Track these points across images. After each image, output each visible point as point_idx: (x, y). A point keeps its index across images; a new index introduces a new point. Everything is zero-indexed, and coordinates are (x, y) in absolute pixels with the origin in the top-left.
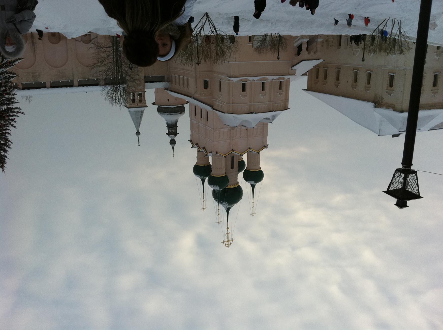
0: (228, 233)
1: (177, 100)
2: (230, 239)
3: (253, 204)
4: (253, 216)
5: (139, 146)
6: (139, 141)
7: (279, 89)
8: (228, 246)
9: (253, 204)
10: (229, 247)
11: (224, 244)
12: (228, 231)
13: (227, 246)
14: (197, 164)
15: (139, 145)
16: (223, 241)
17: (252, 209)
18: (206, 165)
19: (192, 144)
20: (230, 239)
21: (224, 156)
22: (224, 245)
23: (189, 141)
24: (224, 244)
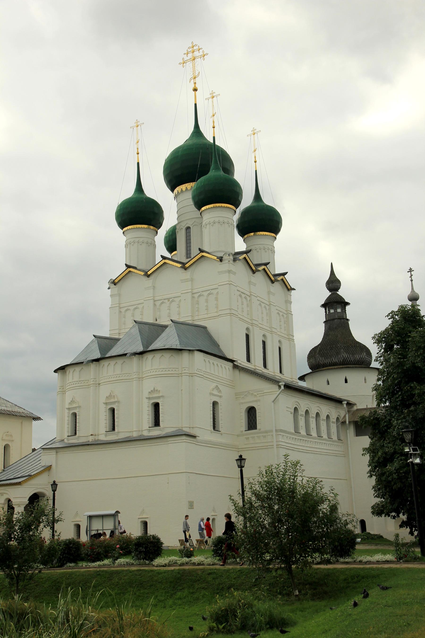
1: (326, 383)
2: (189, 65)
3: (138, 148)
4: (137, 121)
5: (411, 269)
6: (412, 281)
7: (77, 414)
9: (138, 148)
10: (191, 45)
11: (203, 51)
13: (195, 48)
14: (273, 235)
15: (411, 270)
18: (252, 234)
19: (284, 283)
21: (204, 254)
23: (294, 289)
24: (203, 51)
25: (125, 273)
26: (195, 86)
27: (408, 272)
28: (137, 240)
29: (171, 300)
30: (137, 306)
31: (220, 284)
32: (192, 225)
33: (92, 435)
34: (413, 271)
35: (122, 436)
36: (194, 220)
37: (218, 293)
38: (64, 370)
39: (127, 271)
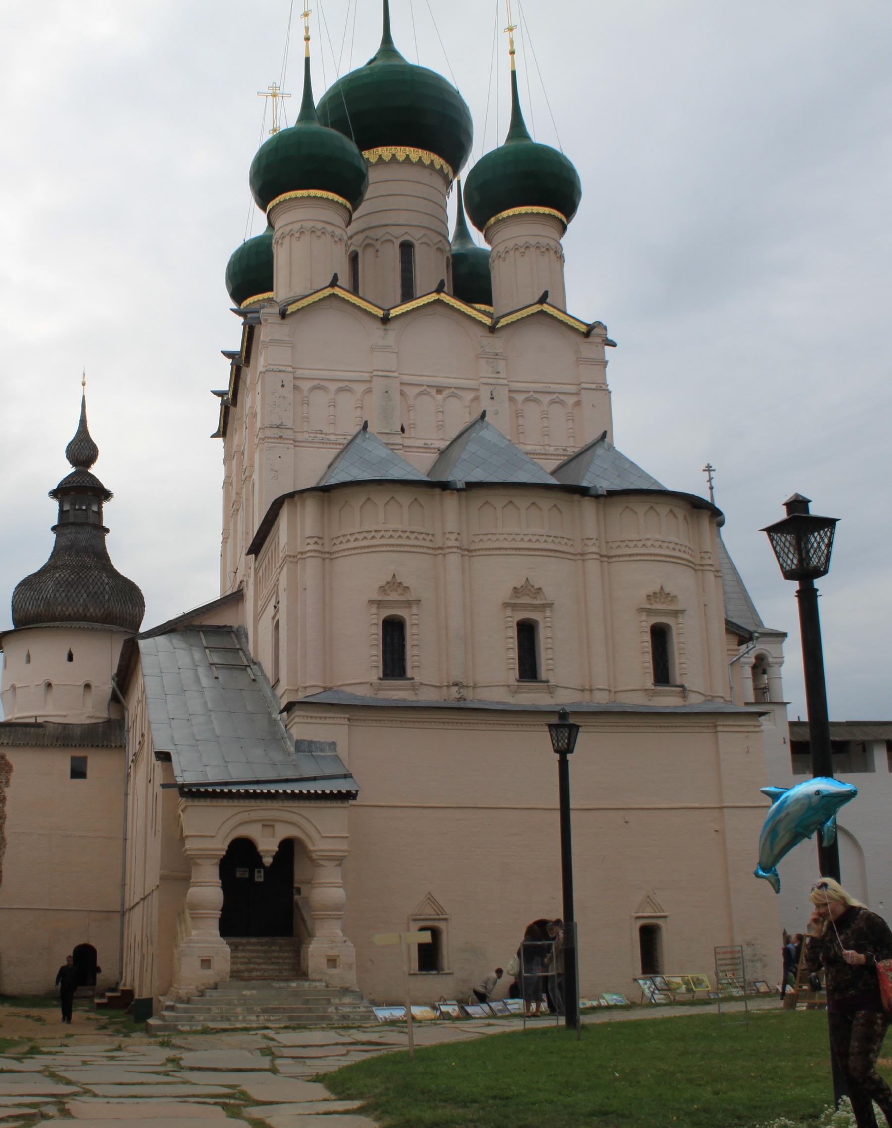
6: (711, 488)
15: (709, 469)
27: (704, 471)
28: (329, 228)
29: (445, 393)
30: (347, 383)
31: (584, 385)
32: (420, 242)
34: (714, 471)
36: (424, 232)
37: (578, 404)
38: (326, 494)
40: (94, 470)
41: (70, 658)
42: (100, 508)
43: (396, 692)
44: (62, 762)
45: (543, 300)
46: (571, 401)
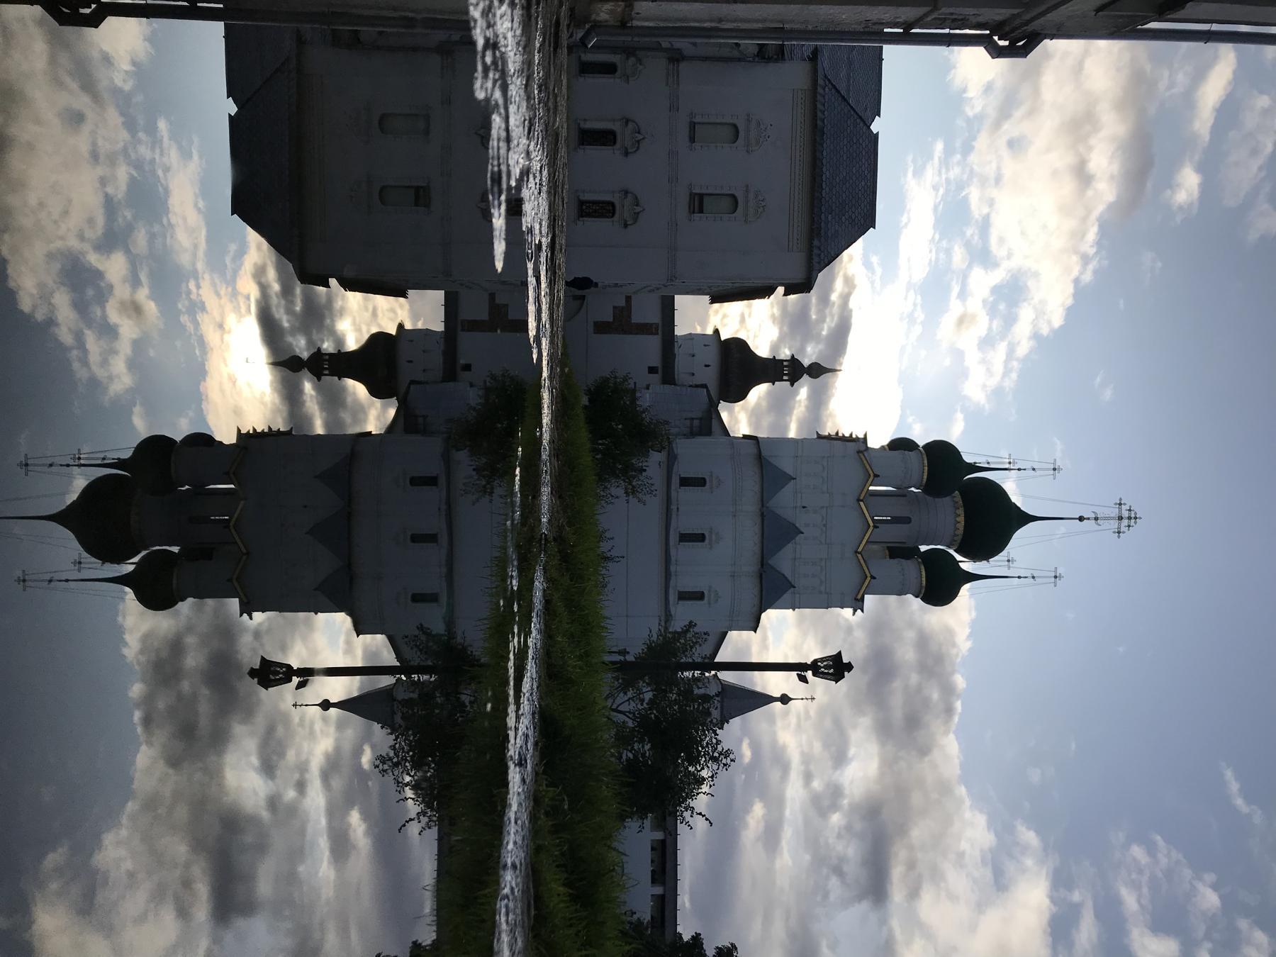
0: (1096, 519)
3: (1025, 469)
4: (1060, 469)
6: (802, 699)
8: (1136, 518)
11: (1124, 532)
12: (1088, 519)
16: (1114, 532)
17: (1038, 473)
20: (1115, 513)
21: (869, 578)
22: (1129, 530)
24: (1124, 532)
25: (869, 469)
26: (1085, 519)
33: (678, 508)
35: (673, 552)
37: (821, 592)
39: (871, 472)
40: (805, 377)
41: (706, 366)
42: (785, 380)
43: (675, 481)
44: (656, 361)
45: (873, 577)
46: (823, 588)
